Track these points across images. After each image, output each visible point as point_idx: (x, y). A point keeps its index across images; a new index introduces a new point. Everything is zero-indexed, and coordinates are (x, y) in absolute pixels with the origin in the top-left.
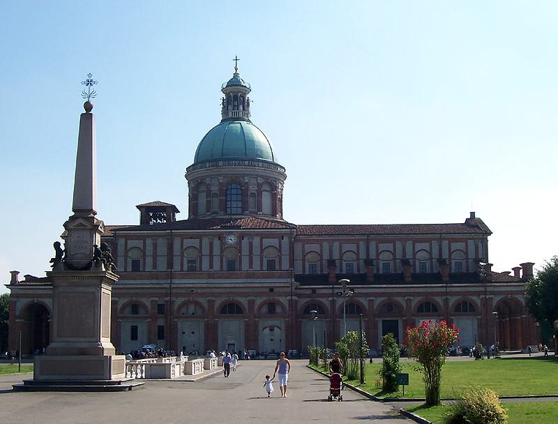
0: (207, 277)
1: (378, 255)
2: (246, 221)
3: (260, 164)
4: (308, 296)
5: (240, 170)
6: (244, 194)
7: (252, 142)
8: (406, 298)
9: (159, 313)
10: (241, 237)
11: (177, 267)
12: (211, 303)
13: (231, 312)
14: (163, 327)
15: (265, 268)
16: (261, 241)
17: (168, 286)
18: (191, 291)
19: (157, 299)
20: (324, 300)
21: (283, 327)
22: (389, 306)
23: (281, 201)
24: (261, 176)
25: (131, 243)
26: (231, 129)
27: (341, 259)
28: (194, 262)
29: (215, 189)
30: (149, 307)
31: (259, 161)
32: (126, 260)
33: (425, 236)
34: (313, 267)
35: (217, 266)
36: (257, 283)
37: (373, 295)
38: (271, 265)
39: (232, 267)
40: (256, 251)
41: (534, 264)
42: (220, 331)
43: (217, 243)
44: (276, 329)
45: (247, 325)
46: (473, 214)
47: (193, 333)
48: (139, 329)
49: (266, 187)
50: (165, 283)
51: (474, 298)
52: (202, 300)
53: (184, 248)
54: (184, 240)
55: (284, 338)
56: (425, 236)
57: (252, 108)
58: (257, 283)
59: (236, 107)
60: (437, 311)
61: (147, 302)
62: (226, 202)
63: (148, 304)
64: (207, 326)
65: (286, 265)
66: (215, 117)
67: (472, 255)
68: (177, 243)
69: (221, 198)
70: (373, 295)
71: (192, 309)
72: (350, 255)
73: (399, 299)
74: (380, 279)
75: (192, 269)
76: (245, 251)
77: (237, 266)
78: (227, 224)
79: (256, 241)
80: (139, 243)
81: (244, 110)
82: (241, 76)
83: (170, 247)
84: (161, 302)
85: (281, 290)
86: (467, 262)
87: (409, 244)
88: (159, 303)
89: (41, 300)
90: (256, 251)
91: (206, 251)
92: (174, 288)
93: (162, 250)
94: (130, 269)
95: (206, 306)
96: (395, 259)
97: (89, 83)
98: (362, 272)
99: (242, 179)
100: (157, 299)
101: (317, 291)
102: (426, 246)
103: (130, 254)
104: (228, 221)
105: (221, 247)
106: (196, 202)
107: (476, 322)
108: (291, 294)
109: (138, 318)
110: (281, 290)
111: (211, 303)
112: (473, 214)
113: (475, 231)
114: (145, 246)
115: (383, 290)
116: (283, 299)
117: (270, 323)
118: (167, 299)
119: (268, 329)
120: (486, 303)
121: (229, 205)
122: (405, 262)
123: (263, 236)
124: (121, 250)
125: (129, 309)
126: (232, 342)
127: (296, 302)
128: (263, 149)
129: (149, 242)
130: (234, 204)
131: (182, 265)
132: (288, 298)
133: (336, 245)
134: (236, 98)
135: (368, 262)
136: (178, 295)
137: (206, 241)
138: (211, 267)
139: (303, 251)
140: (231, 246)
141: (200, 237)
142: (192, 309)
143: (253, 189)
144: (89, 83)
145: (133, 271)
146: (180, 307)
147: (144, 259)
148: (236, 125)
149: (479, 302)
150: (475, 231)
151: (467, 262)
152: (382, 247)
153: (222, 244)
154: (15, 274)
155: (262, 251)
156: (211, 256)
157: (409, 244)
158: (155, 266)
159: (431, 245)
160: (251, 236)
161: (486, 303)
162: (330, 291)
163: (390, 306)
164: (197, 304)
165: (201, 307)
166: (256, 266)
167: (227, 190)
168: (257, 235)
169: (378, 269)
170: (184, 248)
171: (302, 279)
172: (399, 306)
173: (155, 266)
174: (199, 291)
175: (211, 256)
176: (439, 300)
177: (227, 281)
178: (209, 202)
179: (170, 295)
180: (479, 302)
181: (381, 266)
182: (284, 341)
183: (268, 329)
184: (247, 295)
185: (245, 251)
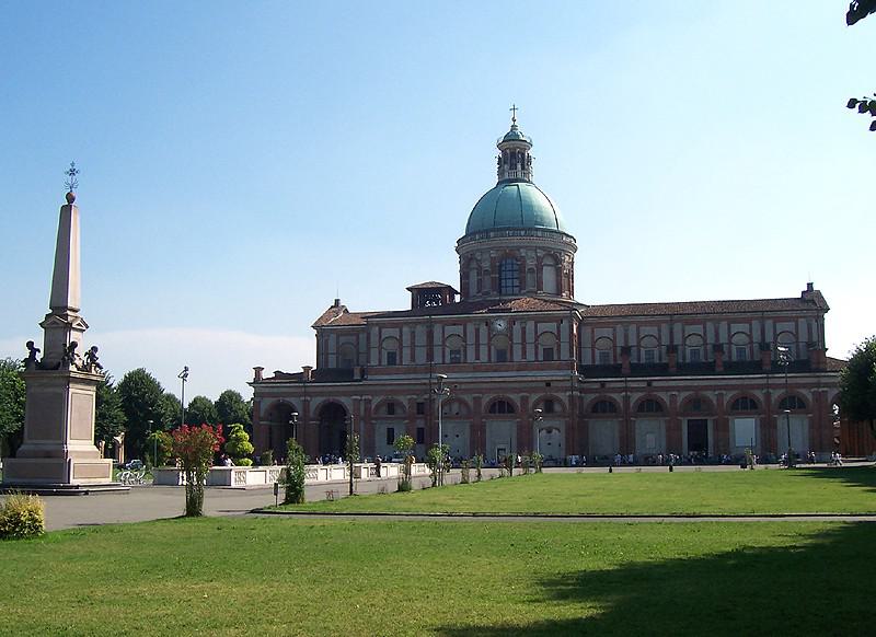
1: (685, 339)
2: (521, 304)
3: (539, 234)
4: (596, 391)
5: (515, 241)
6: (522, 269)
7: (530, 207)
9: (418, 413)
10: (512, 322)
11: (438, 359)
12: (477, 400)
13: (501, 411)
15: (541, 358)
16: (536, 327)
17: (427, 381)
18: (454, 386)
19: (415, 397)
20: (614, 396)
21: (563, 429)
22: (696, 403)
23: (570, 276)
24: (540, 248)
25: (386, 332)
26: (505, 194)
27: (639, 346)
28: (458, 352)
29: (486, 265)
31: (537, 229)
32: (380, 353)
33: (744, 316)
34: (604, 355)
35: (484, 357)
36: (530, 375)
37: (674, 389)
38: (548, 354)
39: (502, 356)
40: (530, 338)
42: (488, 435)
43: (483, 329)
45: (520, 428)
46: (810, 285)
49: (549, 261)
50: (423, 378)
51: (804, 391)
52: (468, 398)
54: (446, 328)
56: (744, 316)
57: (535, 167)
58: (530, 375)
59: (513, 167)
60: (756, 408)
61: (404, 399)
62: (500, 280)
63: (405, 403)
64: (473, 429)
65: (565, 355)
66: (490, 180)
67: (803, 337)
68: (437, 330)
70: (674, 389)
71: (455, 407)
72: (649, 345)
73: (709, 394)
74: (684, 369)
75: (455, 361)
76: (517, 338)
77: (508, 355)
78: (493, 306)
79: (530, 325)
80: (395, 332)
81: (523, 168)
82: (519, 129)
83: (430, 335)
85: (560, 384)
86: (797, 346)
87: (723, 326)
89: (287, 399)
90: (530, 338)
91: (471, 339)
93: (421, 339)
94: (385, 362)
95: (471, 403)
96: (705, 344)
97: (72, 172)
98: (664, 361)
100: (415, 397)
101: (607, 385)
102: (744, 327)
103: (384, 345)
104: (496, 303)
105: (489, 334)
107: (806, 422)
108: (572, 389)
109: (395, 418)
110: (560, 384)
111: (477, 400)
112: (810, 285)
113: (811, 305)
114: (401, 336)
115: (688, 383)
116: (561, 395)
117: (548, 424)
118: (426, 396)
119: (544, 431)
120: (819, 397)
121: (503, 284)
122: (718, 348)
123: (538, 320)
124: (374, 340)
125: (384, 409)
126: (502, 446)
127: (581, 398)
128: (544, 215)
129: (406, 329)
130: (509, 283)
131: (444, 357)
132: (568, 394)
133: (633, 328)
134: (513, 155)
135: (672, 349)
137: (471, 328)
139: (593, 338)
140: (500, 333)
141: (464, 323)
142: (455, 407)
143: (530, 263)
144: (72, 172)
145: (389, 363)
147: (401, 353)
148: (512, 189)
149: (810, 397)
150: (811, 305)
151: (797, 346)
152: (690, 329)
154: (258, 370)
155: (537, 338)
156: (478, 345)
157: (723, 326)
158: (413, 358)
159: (751, 325)
160: (524, 320)
161: (819, 397)
162: (623, 385)
163: (696, 403)
164: (462, 402)
165: (466, 404)
166: (531, 357)
167: (501, 266)
168: (530, 318)
169: (684, 358)
171: (586, 371)
172: (707, 401)
173: (413, 358)
174: (463, 387)
175: (478, 345)
176: (759, 394)
177: (496, 374)
178: (480, 282)
180: (810, 397)
181: (688, 350)
182: (563, 446)
183: (544, 431)
184: (520, 390)
185: (517, 338)
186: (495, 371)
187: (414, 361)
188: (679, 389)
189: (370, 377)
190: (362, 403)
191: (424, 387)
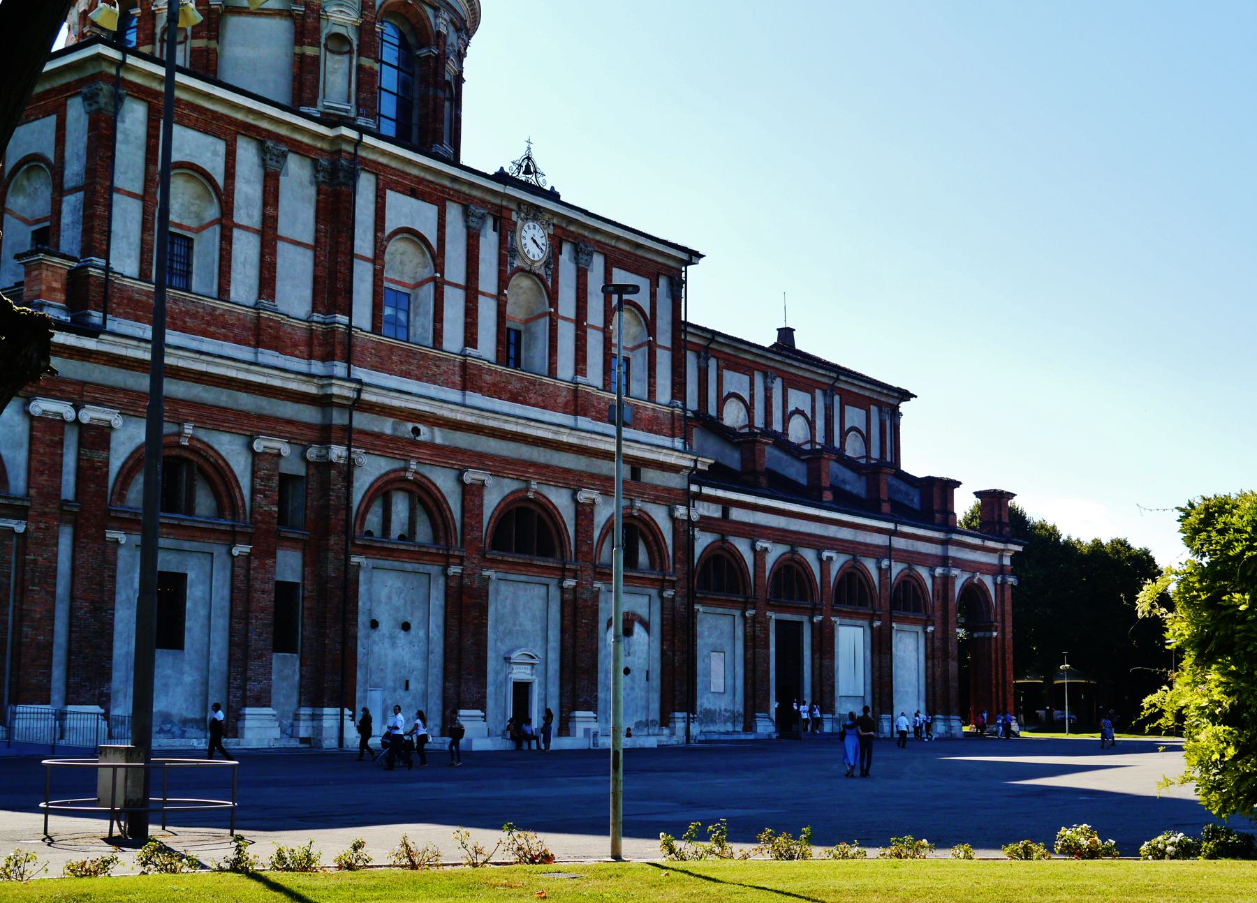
0: (457, 379)
8: (826, 554)
14: (294, 585)
19: (285, 449)
30: (245, 482)
41: (1015, 495)
44: (638, 628)
47: (406, 627)
48: (195, 593)
52: (444, 481)
53: (388, 231)
55: (656, 667)
63: (240, 464)
69: (366, 62)
77: (537, 354)
84: (292, 464)
88: (285, 467)
92: (372, 408)
99: (430, 12)
106: (213, 44)
111: (471, 493)
136: (378, 444)
138: (471, 338)
146: (369, 498)
153: (507, 251)
170: (388, 231)
174: (439, 437)
179: (348, 436)
184: (572, 481)
186: (514, 398)
187: (272, 297)
188: (779, 536)
189: (114, 324)
190: (71, 439)
191: (309, 414)
